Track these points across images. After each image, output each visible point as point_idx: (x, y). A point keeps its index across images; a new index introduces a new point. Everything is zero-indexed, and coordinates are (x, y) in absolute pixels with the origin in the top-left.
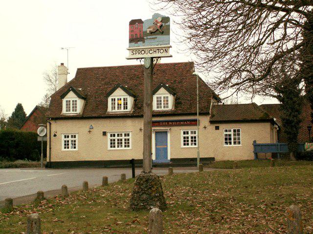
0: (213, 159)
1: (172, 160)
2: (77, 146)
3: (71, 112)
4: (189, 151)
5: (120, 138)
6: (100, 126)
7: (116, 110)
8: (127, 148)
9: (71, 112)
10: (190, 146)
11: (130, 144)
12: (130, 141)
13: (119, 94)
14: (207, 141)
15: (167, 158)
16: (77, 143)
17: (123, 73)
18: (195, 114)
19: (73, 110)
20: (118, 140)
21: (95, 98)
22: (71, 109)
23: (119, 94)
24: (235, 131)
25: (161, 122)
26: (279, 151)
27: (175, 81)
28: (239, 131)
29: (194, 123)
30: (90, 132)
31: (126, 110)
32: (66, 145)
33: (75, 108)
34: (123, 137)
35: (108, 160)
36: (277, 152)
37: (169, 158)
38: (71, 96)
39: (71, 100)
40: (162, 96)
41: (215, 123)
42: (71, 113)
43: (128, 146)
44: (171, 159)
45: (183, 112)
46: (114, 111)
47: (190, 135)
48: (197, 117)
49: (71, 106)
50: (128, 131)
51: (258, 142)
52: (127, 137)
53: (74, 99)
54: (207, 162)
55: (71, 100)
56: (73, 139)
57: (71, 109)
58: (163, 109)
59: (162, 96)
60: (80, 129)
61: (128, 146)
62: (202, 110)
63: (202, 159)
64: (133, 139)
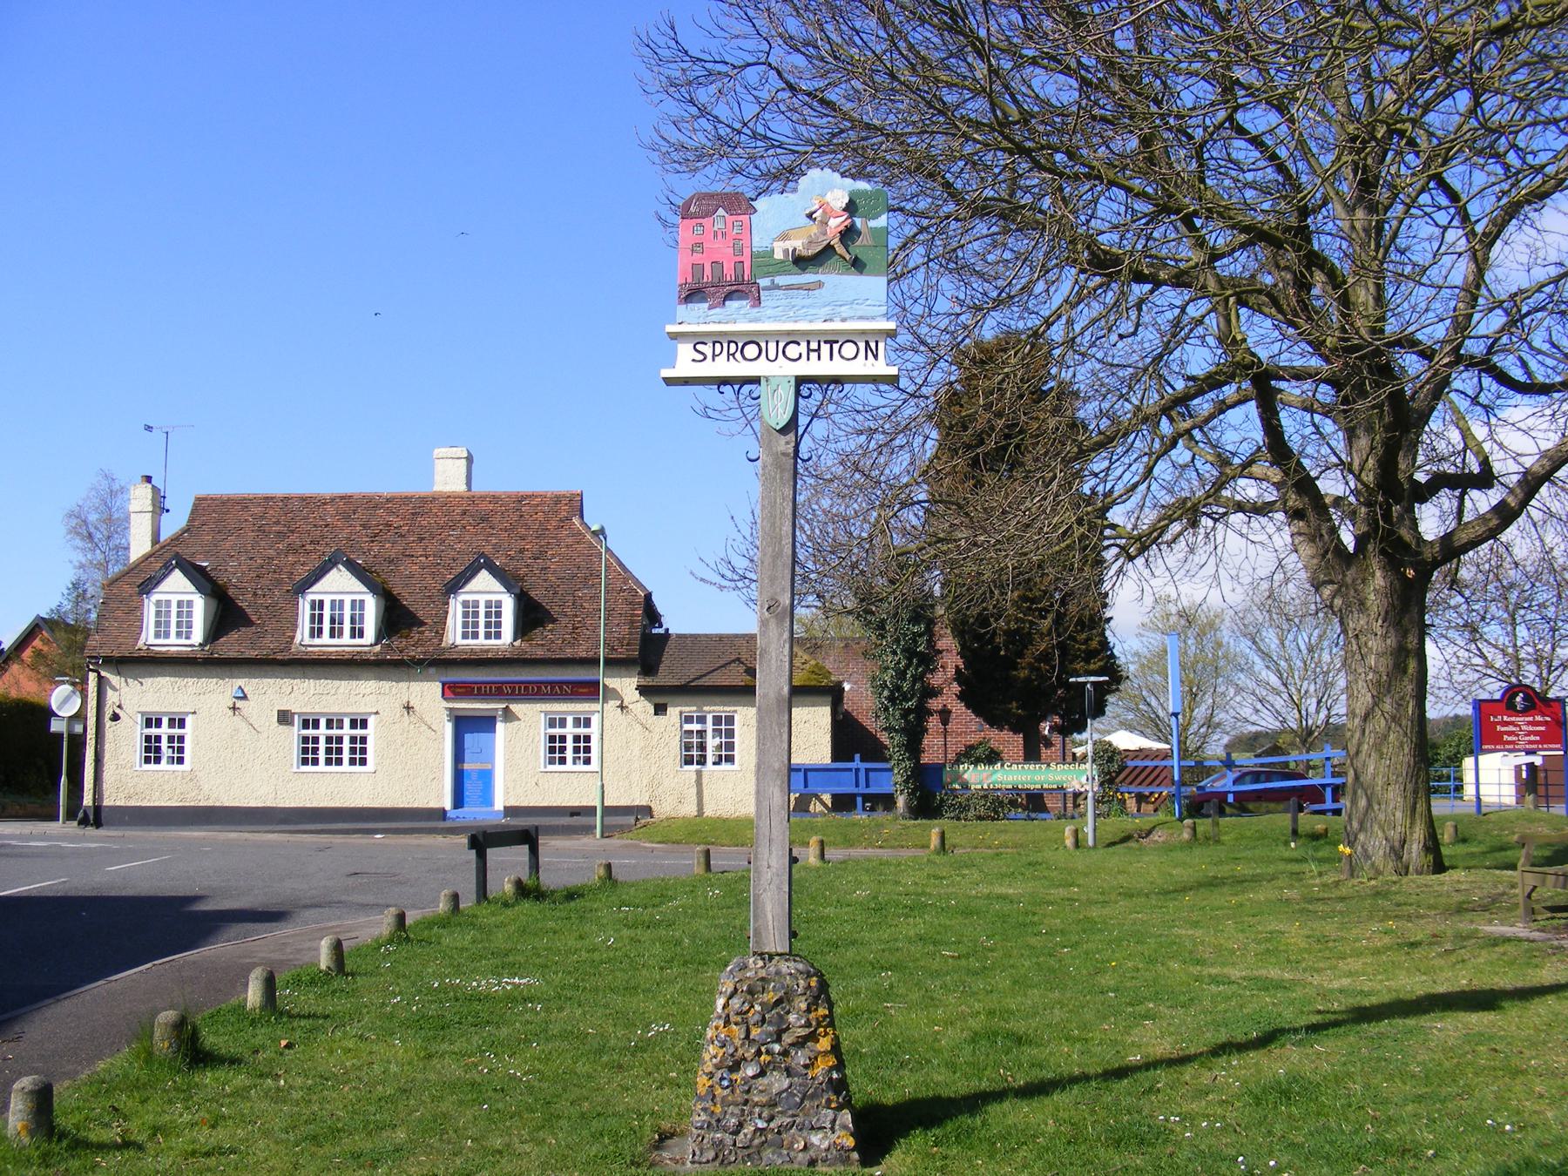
0: (647, 811)
1: (510, 811)
2: (187, 755)
3: (173, 639)
4: (569, 787)
5: (335, 732)
8: (357, 768)
10: (569, 766)
11: (370, 756)
12: (370, 746)
13: (339, 585)
14: (631, 752)
15: (492, 804)
16: (187, 745)
18: (594, 662)
19: (179, 634)
21: (255, 594)
22: (173, 629)
23: (339, 585)
24: (717, 720)
25: (481, 687)
26: (862, 790)
27: (522, 551)
28: (730, 720)
29: (590, 691)
30: (234, 708)
31: (358, 641)
32: (152, 752)
33: (185, 628)
34: (347, 732)
36: (855, 791)
37: (499, 805)
38: (177, 586)
40: (482, 599)
41: (659, 696)
42: (173, 644)
43: (363, 762)
44: (506, 808)
45: (549, 655)
47: (570, 730)
52: (359, 732)
56: (176, 731)
58: (481, 640)
59: (482, 599)
60: (201, 699)
61: (363, 762)
62: (613, 649)
63: (609, 811)
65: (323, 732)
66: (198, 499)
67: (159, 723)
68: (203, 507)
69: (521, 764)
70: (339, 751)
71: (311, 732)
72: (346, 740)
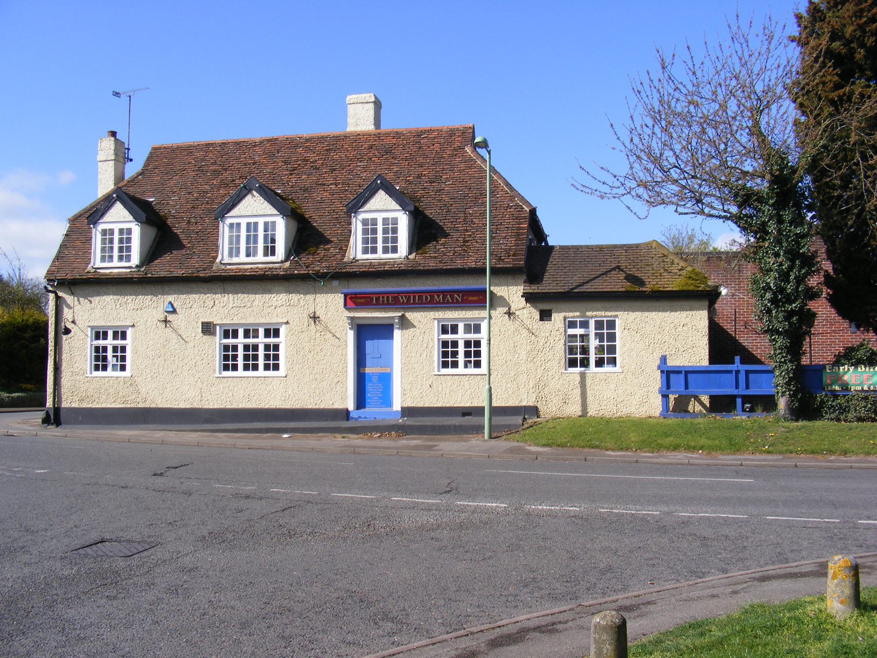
0: (534, 411)
1: (407, 412)
2: (128, 363)
3: (116, 263)
4: (461, 389)
5: (251, 341)
6: (197, 307)
7: (242, 258)
8: (271, 373)
9: (116, 263)
10: (461, 369)
11: (282, 362)
12: (282, 353)
13: (254, 208)
14: (519, 353)
15: (390, 405)
16: (128, 354)
17: (271, 155)
18: (481, 272)
19: (121, 258)
20: (246, 347)
21: (189, 222)
22: (116, 253)
23: (254, 208)
24: (599, 325)
25: (379, 297)
26: (742, 391)
27: (419, 177)
28: (612, 325)
29: (476, 299)
30: (166, 321)
31: (270, 259)
32: (100, 361)
33: (125, 252)
34: (241, 340)
35: (216, 406)
36: (735, 392)
37: (397, 406)
38: (119, 217)
39: (116, 227)
40: (380, 217)
41: (544, 303)
42: (116, 266)
43: (276, 367)
44: (402, 408)
45: (440, 266)
46: (235, 260)
47: (461, 336)
48: (486, 282)
49: (116, 245)
50: (274, 320)
51: (672, 363)
52: (272, 340)
53: (125, 226)
54: (518, 418)
55: (116, 227)
56: (119, 342)
57: (116, 253)
58: (380, 255)
59: (380, 217)
60: (138, 313)
61: (276, 367)
62: (500, 259)
63: (496, 411)
64: (135, 352)
65: (241, 340)
66: (154, 149)
67: (235, 335)
68: (157, 155)
69: (415, 366)
70: (256, 358)
71: (230, 341)
72: (241, 349)
